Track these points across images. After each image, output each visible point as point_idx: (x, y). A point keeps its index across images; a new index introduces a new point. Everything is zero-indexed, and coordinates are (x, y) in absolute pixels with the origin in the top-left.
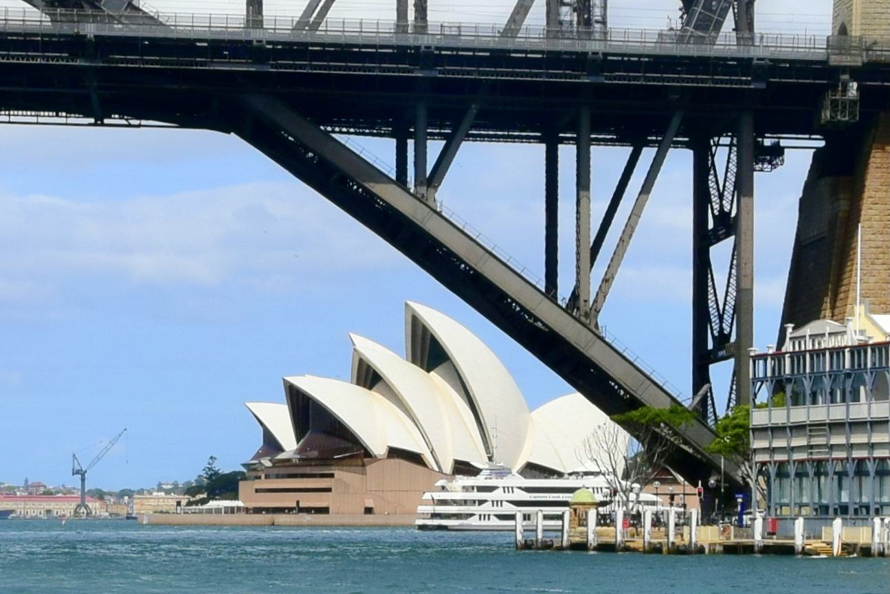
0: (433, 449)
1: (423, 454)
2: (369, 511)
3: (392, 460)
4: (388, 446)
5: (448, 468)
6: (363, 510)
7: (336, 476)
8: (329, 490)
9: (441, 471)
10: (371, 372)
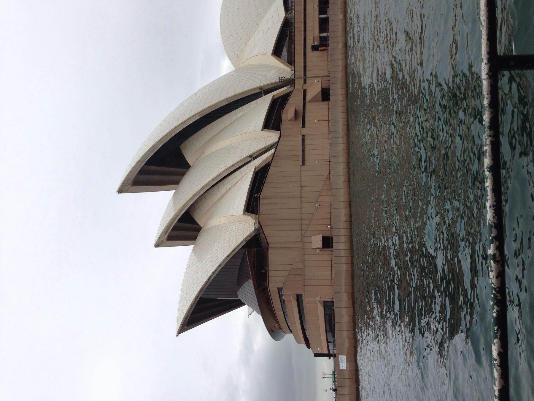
0: (250, 156)
1: (256, 168)
2: (327, 242)
3: (261, 208)
4: (244, 214)
5: (272, 137)
6: (327, 251)
7: (280, 286)
8: (299, 298)
9: (275, 145)
10: (181, 224)
